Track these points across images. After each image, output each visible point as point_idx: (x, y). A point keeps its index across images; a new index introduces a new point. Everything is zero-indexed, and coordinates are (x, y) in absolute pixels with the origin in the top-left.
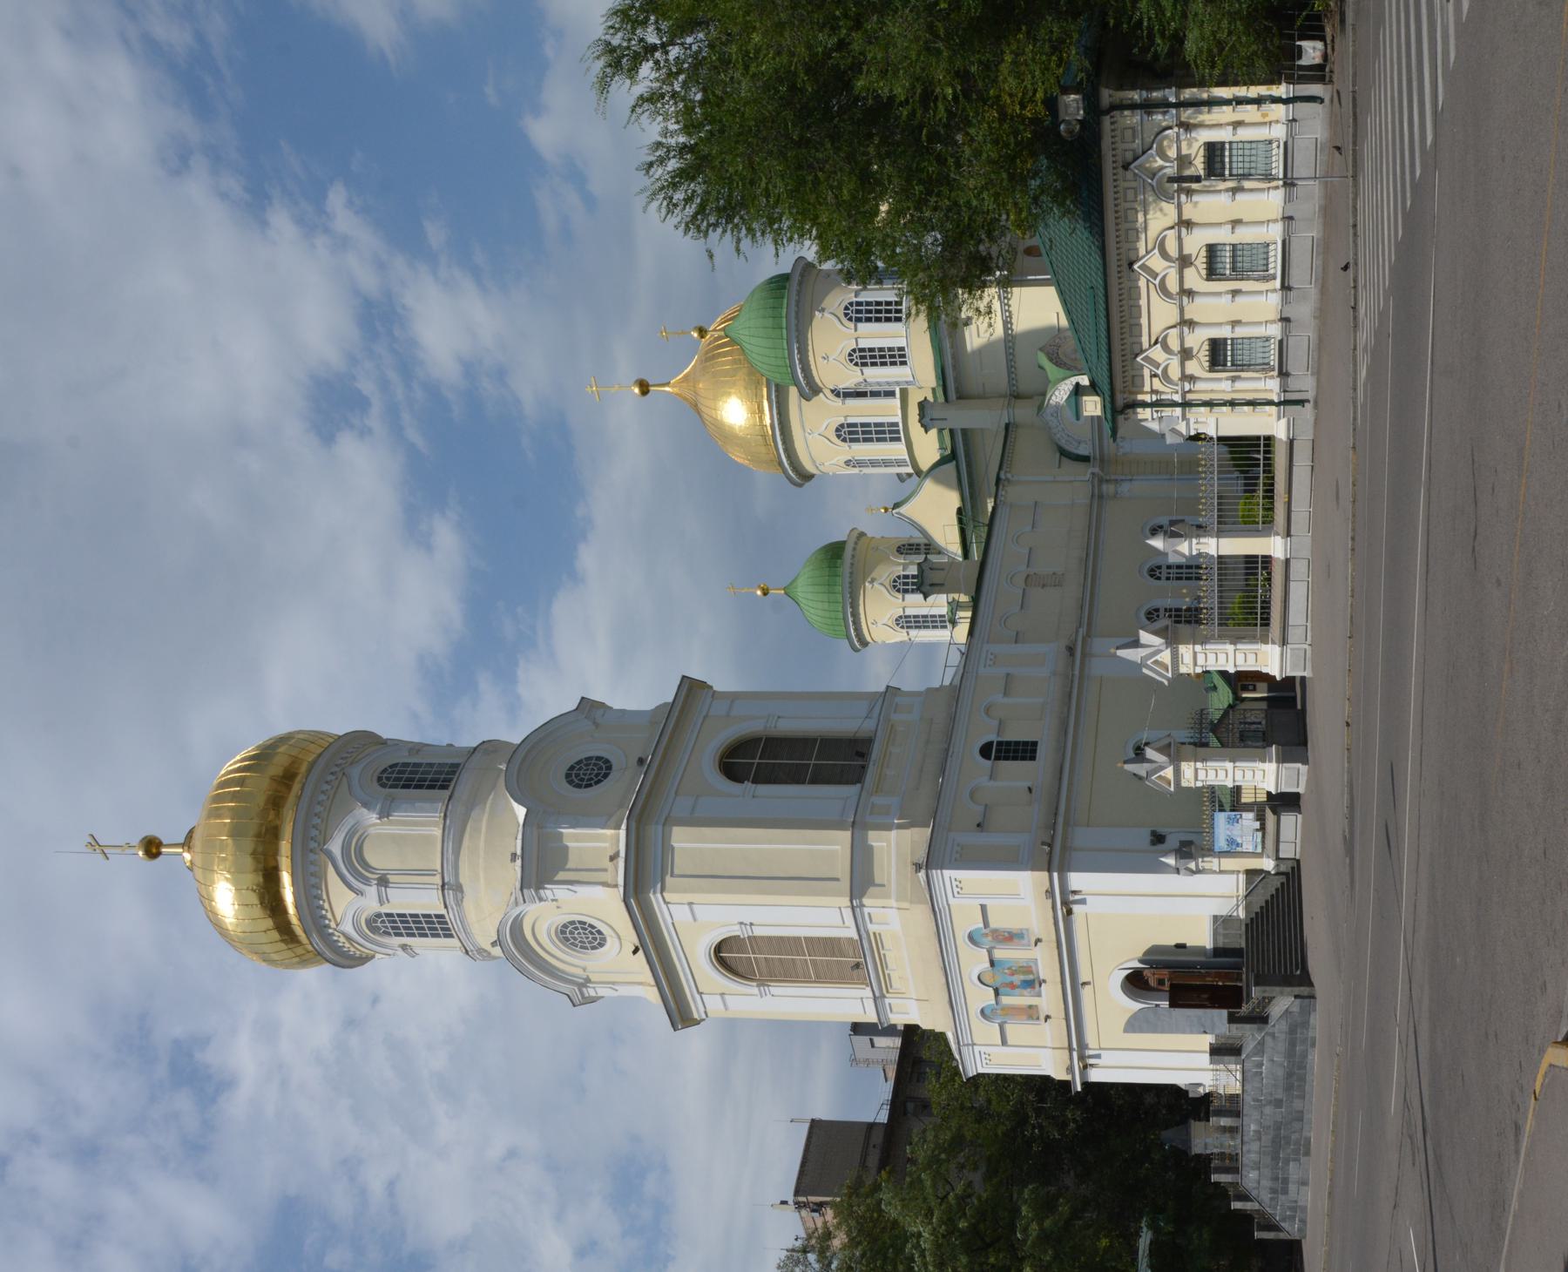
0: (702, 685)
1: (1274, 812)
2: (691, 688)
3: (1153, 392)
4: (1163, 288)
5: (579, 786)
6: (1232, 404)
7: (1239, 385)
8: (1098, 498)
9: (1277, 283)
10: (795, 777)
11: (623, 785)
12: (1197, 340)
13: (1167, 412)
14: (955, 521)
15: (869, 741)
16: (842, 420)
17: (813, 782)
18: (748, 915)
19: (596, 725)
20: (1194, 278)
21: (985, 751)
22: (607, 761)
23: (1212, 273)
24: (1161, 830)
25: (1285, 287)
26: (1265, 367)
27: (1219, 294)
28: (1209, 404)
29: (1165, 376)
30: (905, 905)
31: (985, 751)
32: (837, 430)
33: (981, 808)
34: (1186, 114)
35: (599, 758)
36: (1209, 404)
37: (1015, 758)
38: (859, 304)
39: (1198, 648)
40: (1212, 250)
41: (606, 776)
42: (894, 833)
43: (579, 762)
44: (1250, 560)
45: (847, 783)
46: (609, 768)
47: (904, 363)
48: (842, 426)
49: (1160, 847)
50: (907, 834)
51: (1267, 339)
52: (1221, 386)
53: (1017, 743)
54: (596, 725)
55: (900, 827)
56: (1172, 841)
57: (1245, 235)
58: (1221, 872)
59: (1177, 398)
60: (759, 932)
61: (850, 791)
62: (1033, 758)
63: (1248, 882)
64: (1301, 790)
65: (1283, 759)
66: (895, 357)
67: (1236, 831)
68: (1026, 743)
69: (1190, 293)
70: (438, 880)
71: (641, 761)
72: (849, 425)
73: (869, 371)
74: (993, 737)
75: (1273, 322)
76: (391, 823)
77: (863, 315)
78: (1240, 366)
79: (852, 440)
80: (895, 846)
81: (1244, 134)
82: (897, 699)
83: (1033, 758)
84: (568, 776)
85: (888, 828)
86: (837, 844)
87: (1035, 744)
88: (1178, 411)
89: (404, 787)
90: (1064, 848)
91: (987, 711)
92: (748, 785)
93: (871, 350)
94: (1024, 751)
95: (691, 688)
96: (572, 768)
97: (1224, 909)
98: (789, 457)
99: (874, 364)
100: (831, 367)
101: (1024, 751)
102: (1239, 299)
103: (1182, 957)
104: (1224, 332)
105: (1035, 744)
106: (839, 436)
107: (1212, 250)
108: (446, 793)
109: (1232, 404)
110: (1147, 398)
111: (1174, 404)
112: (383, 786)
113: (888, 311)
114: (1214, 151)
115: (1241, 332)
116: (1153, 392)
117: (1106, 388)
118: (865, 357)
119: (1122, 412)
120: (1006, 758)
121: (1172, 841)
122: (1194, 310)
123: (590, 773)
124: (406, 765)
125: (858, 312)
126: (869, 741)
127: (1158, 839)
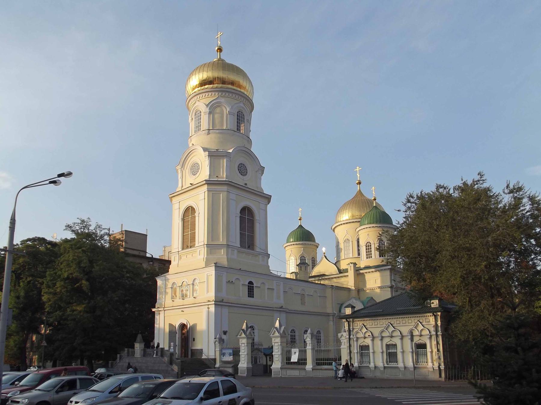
0: (269, 202)
1: (232, 367)
2: (268, 198)
3: (353, 329)
4: (382, 332)
5: (238, 167)
6: (350, 352)
7: (356, 354)
8: (328, 315)
9: (386, 365)
10: (242, 228)
11: (239, 179)
12: (368, 341)
13: (347, 333)
15: (253, 249)
18: (202, 215)
19: (256, 172)
20: (386, 341)
21: (251, 283)
22: (246, 175)
23: (388, 346)
24: (227, 334)
25: (385, 367)
26: (361, 362)
27: (382, 348)
28: (350, 346)
29: (357, 332)
30: (205, 260)
31: (251, 283)
34: (434, 338)
36: (350, 346)
37: (249, 291)
39: (280, 344)
40: (395, 346)
41: (242, 174)
42: (225, 257)
44: (306, 360)
46: (244, 175)
49: (223, 333)
50: (226, 260)
51: (370, 363)
52: (355, 350)
53: (253, 292)
54: (256, 172)
55: (227, 258)
56: (224, 337)
57: (400, 356)
58: (215, 351)
59: (352, 337)
60: (197, 218)
62: (249, 296)
63: (212, 359)
64: (239, 374)
65: (248, 369)
67: (227, 355)
68: (253, 294)
69: (382, 340)
70: (211, 128)
71: (246, 184)
74: (255, 285)
75: (375, 365)
76: (227, 115)
78: (362, 355)
80: (222, 256)
81: (429, 354)
82: (266, 257)
83: (249, 296)
85: (227, 255)
86: (222, 240)
87: (253, 297)
88: (348, 337)
89: (237, 119)
90: (222, 305)
91: (263, 283)
92: (239, 215)
94: (251, 294)
95: (268, 198)
97: (205, 351)
101: (251, 294)
102: (381, 354)
103: (191, 340)
104: (371, 350)
105: (253, 297)
107: (395, 346)
108: (236, 130)
109: (350, 352)
110: (351, 328)
111: (350, 335)
112: (238, 113)
114: (423, 346)
115: (371, 355)
116: (353, 329)
117: (354, 315)
119: (347, 320)
120: (248, 289)
121: (224, 337)
122: (378, 342)
123: (242, 170)
124: (244, 119)
126: (253, 249)
127: (225, 333)
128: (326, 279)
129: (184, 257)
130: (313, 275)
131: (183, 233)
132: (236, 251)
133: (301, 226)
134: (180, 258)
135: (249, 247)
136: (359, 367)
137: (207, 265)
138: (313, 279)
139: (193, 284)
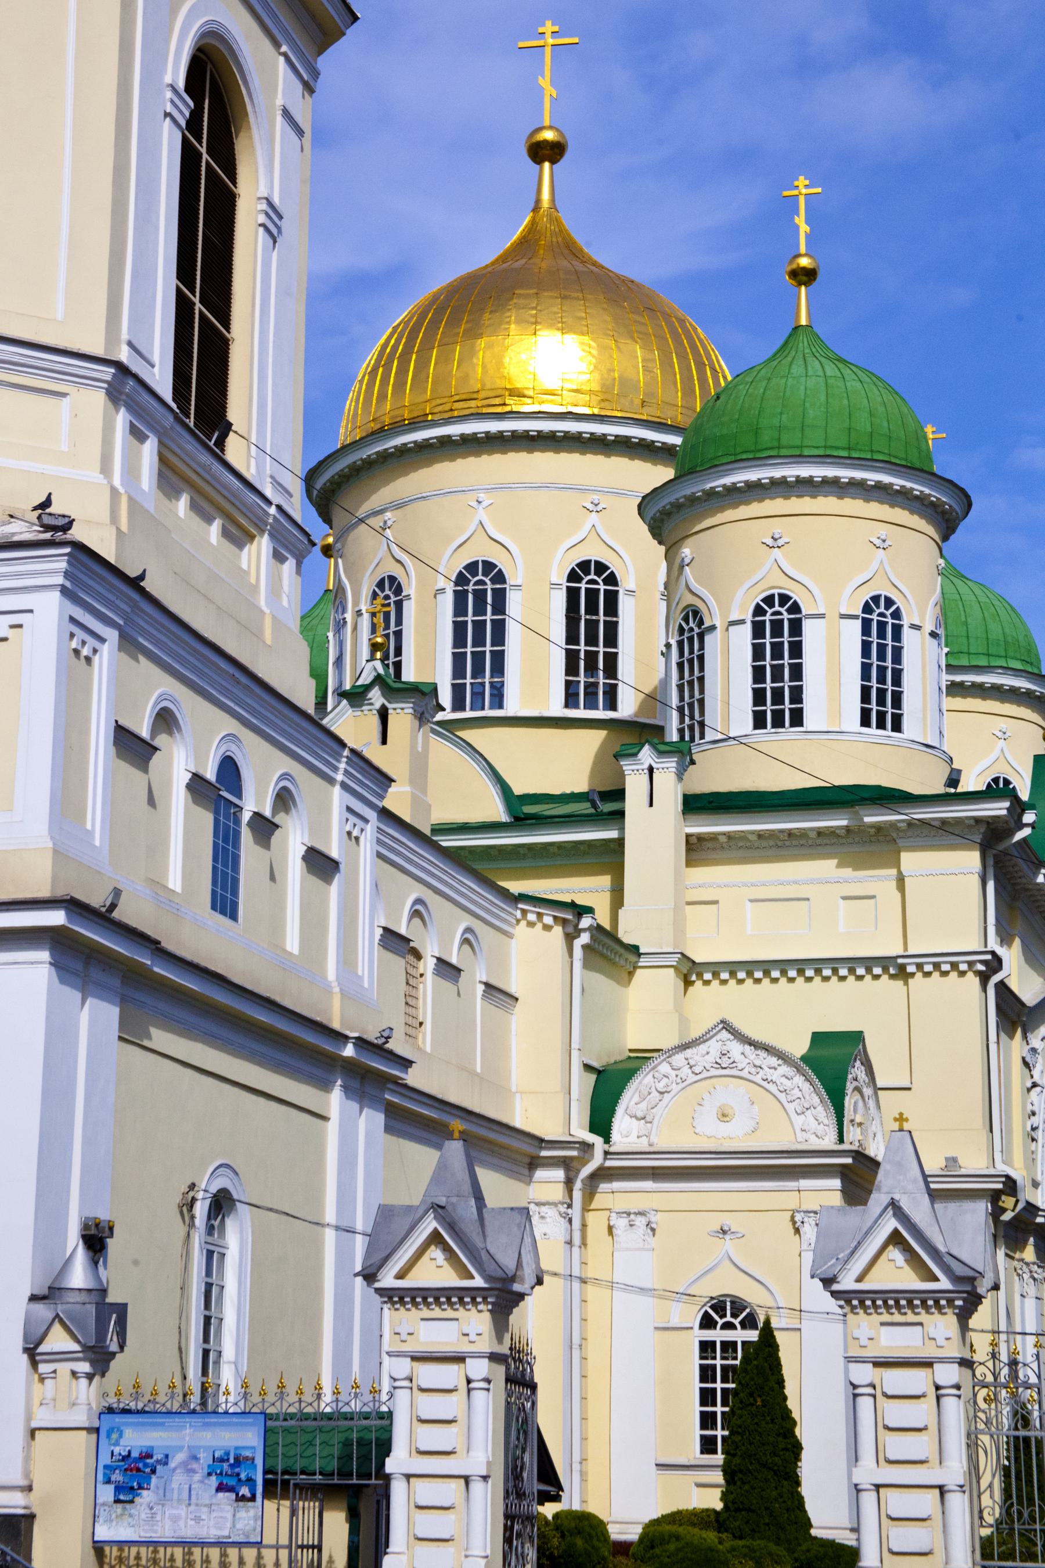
16: (511, 578)
32: (489, 566)
38: (897, 630)
47: (759, 722)
48: (500, 577)
66: (779, 703)
72: (500, 596)
73: (743, 638)
77: (874, 638)
79: (460, 599)
93: (797, 650)
98: (423, 447)
99: (758, 652)
100: (749, 553)
106: (472, 567)
113: (881, 701)
118: (778, 628)
125: (882, 626)
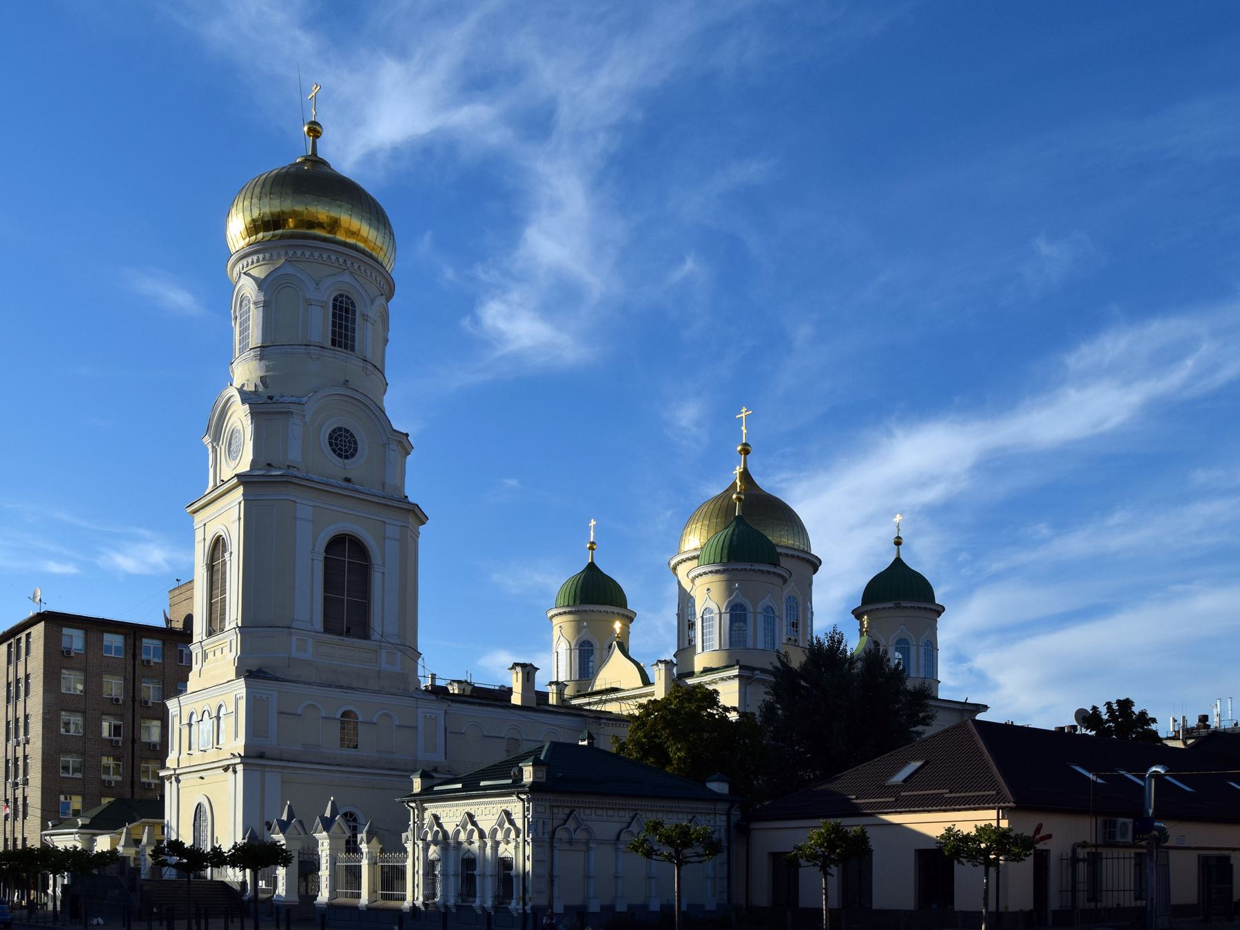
5: (331, 437)
14: (608, 686)
15: (365, 635)
17: (326, 598)
22: (353, 455)
26: (426, 897)
33: (299, 712)
35: (356, 450)
41: (340, 456)
43: (352, 435)
45: (325, 621)
46: (347, 457)
61: (319, 624)
71: (348, 480)
84: (340, 429)
96: (347, 431)
123: (343, 444)
128: (623, 699)
129: (210, 656)
130: (597, 688)
131: (211, 598)
132: (310, 641)
133: (592, 567)
134: (205, 656)
135: (348, 630)
136: (457, 907)
137: (238, 676)
138: (586, 700)
139: (218, 718)
